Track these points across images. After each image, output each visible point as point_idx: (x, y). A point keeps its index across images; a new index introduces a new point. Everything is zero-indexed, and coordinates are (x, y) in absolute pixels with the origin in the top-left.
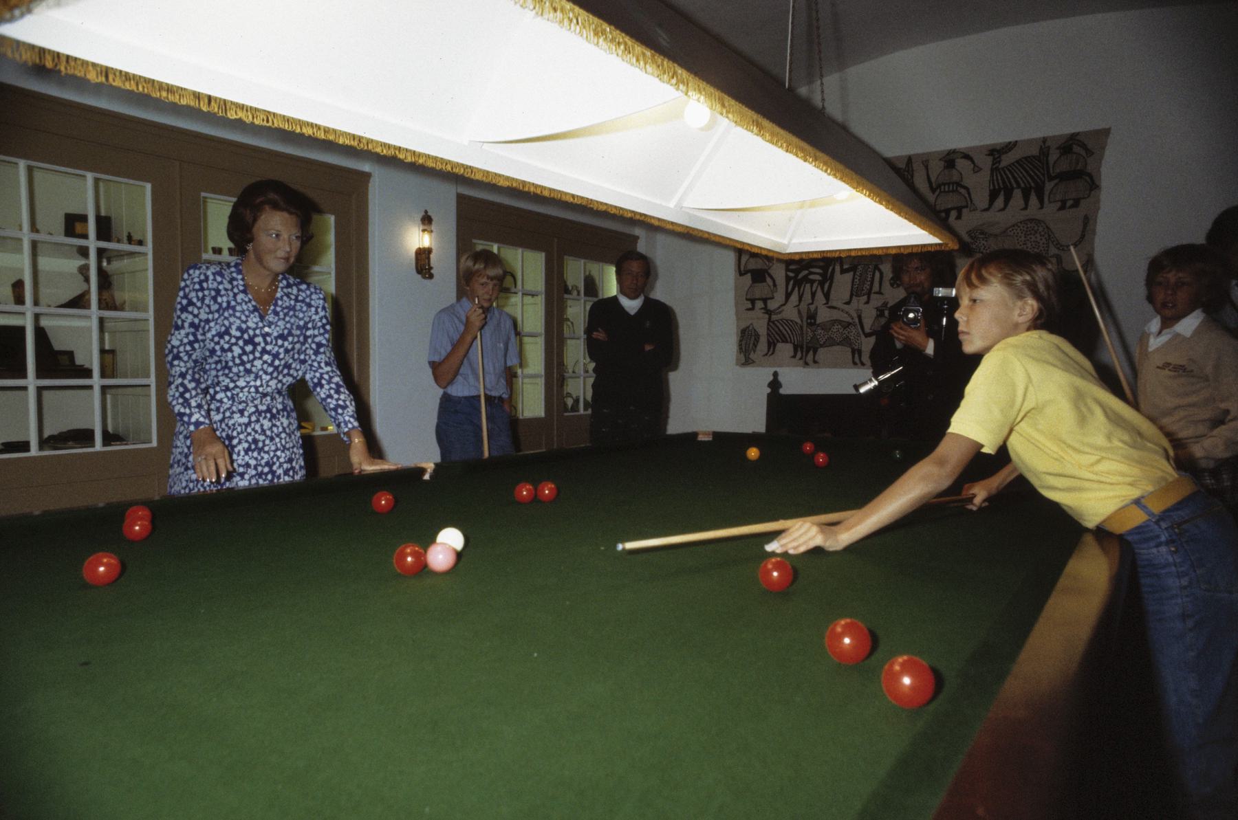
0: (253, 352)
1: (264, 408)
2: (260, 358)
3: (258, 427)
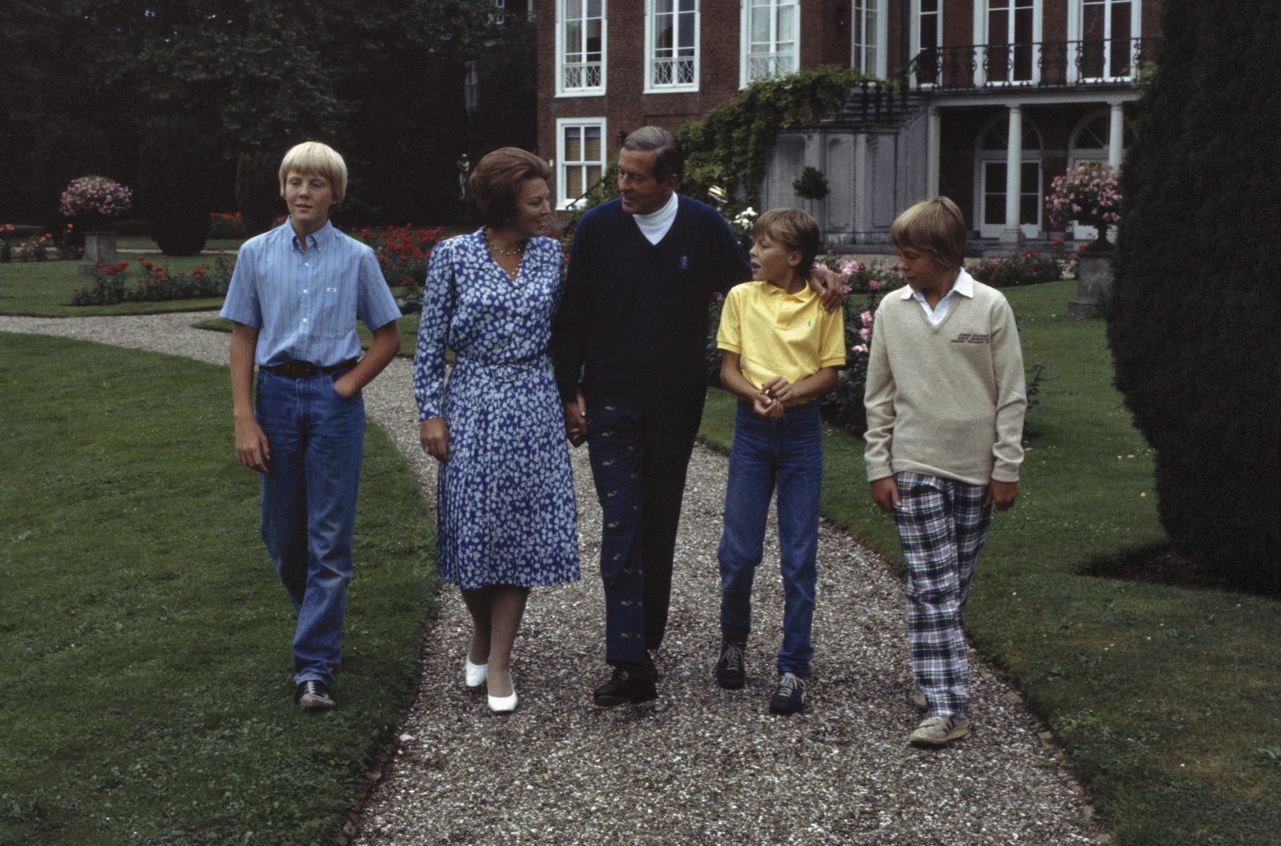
1: (519, 383)
3: (513, 403)
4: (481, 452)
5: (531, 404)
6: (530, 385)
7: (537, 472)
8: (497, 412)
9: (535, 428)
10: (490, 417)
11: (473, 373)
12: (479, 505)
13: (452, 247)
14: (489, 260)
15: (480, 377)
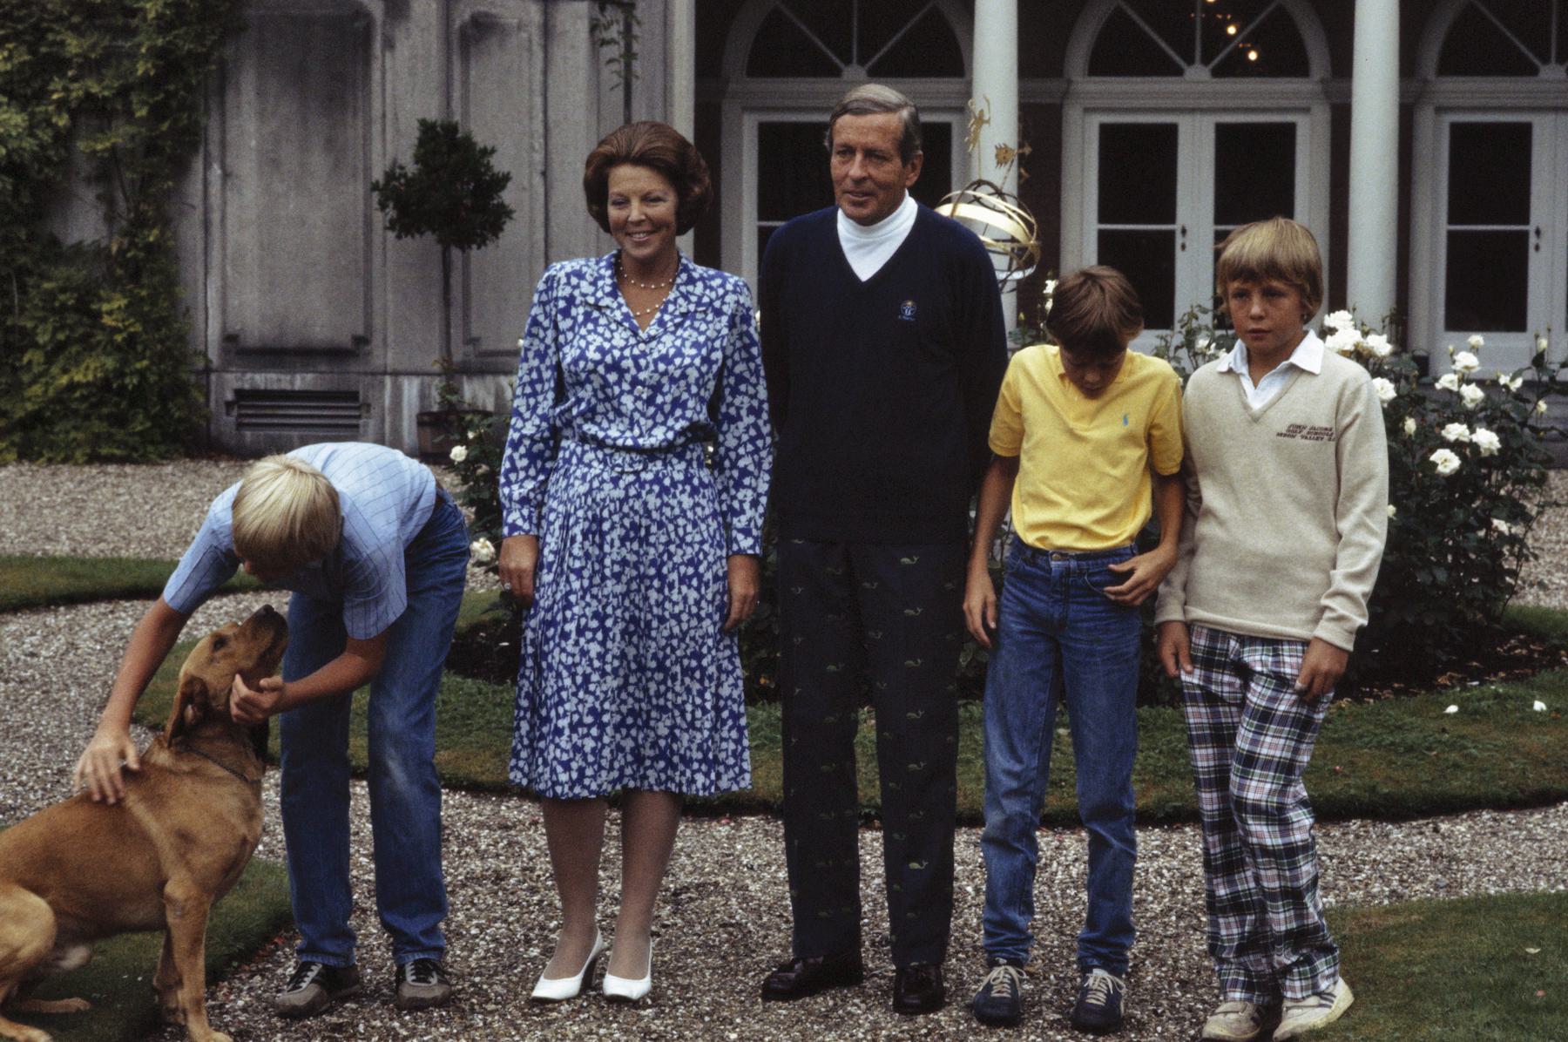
0: (619, 383)
1: (649, 476)
2: (630, 392)
4: (597, 580)
5: (667, 511)
6: (667, 482)
7: (677, 617)
8: (616, 518)
9: (672, 548)
10: (606, 526)
11: (580, 461)
12: (597, 664)
13: (562, 274)
14: (613, 294)
15: (589, 466)
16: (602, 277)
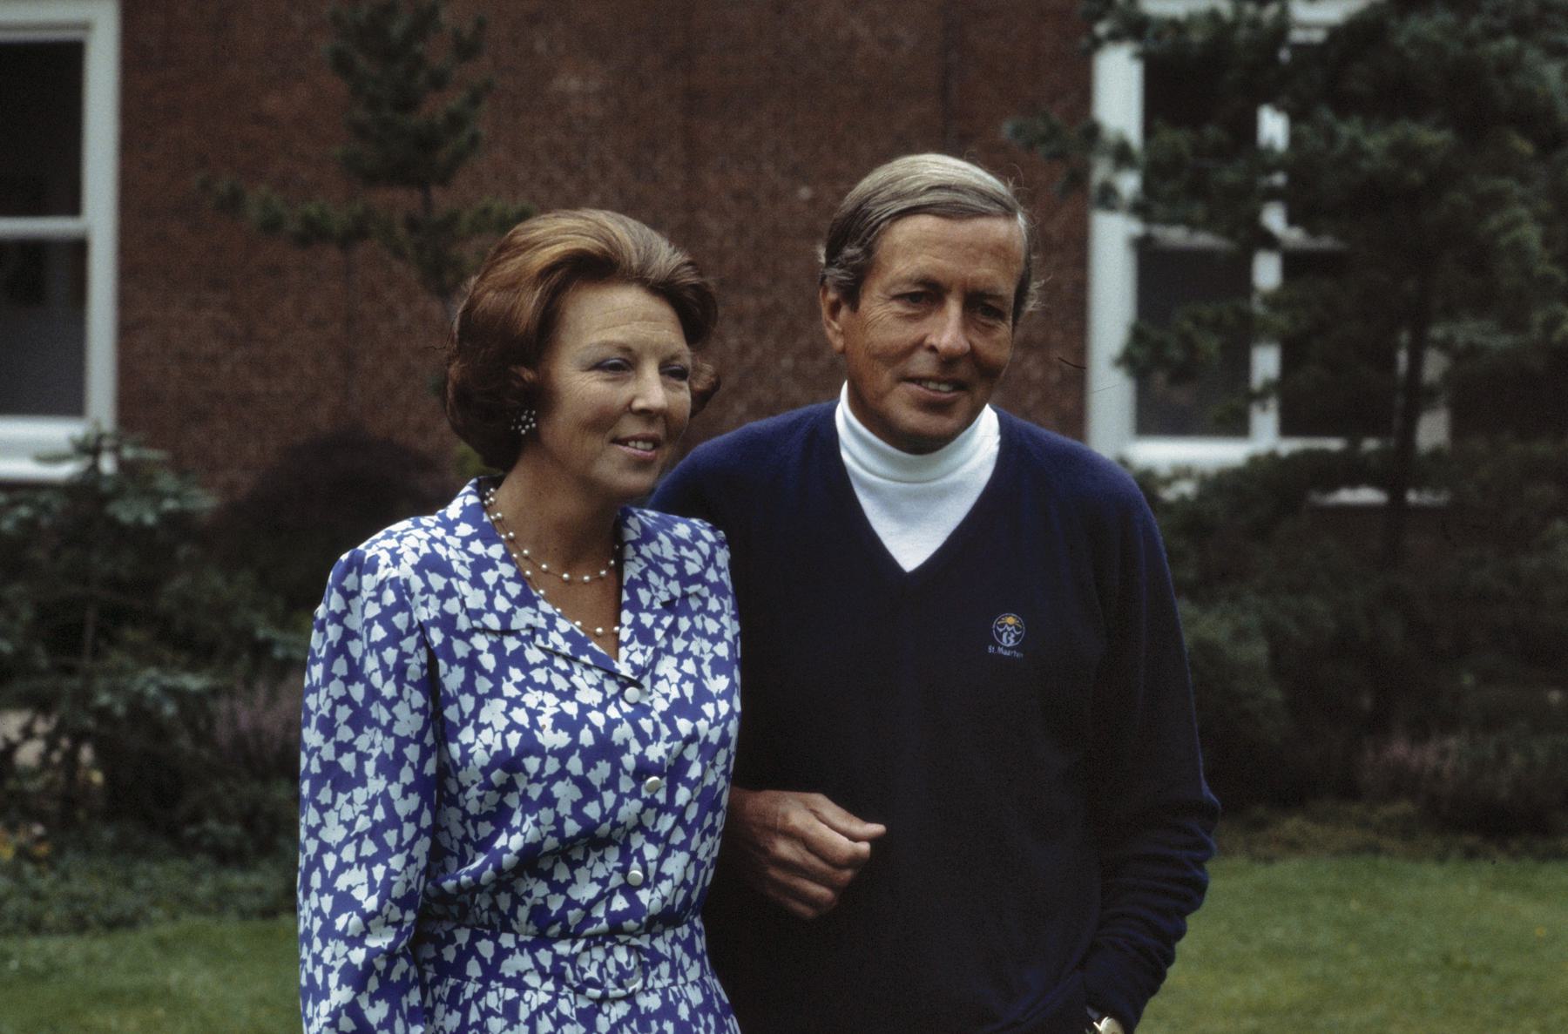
14: (526, 599)
16: (489, 563)
